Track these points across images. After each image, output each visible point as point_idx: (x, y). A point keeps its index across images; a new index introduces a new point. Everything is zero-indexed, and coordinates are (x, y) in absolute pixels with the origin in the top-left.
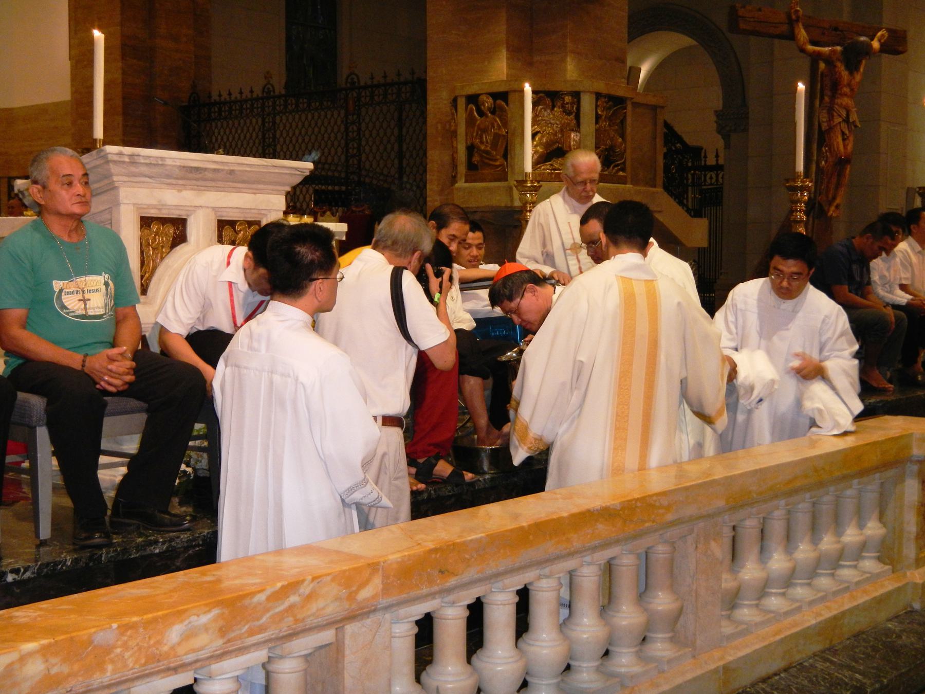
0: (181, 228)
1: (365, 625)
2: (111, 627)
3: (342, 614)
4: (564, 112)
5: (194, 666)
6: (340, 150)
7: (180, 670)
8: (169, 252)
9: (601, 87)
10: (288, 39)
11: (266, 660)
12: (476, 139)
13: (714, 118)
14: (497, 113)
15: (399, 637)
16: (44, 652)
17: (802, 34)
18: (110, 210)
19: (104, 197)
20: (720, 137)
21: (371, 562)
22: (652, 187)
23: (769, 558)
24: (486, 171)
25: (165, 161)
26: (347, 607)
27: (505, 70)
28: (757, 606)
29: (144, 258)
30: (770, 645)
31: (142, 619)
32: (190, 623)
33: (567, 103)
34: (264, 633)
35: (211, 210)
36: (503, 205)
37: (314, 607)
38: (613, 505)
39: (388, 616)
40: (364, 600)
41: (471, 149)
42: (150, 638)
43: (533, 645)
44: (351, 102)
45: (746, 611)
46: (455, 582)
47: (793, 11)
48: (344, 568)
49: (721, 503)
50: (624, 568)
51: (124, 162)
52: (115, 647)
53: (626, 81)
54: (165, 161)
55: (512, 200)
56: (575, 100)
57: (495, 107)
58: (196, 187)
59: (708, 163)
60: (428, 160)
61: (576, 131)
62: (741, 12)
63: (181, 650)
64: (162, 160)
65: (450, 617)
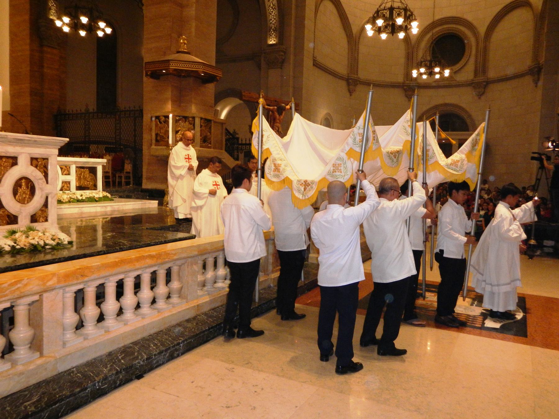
4: (189, 123)
9: (203, 116)
21: (52, 273)
24: (162, 143)
27: (170, 108)
37: (28, 288)
39: (61, 291)
40: (50, 285)
41: (157, 135)
44: (117, 117)
49: (196, 253)
62: (243, 94)
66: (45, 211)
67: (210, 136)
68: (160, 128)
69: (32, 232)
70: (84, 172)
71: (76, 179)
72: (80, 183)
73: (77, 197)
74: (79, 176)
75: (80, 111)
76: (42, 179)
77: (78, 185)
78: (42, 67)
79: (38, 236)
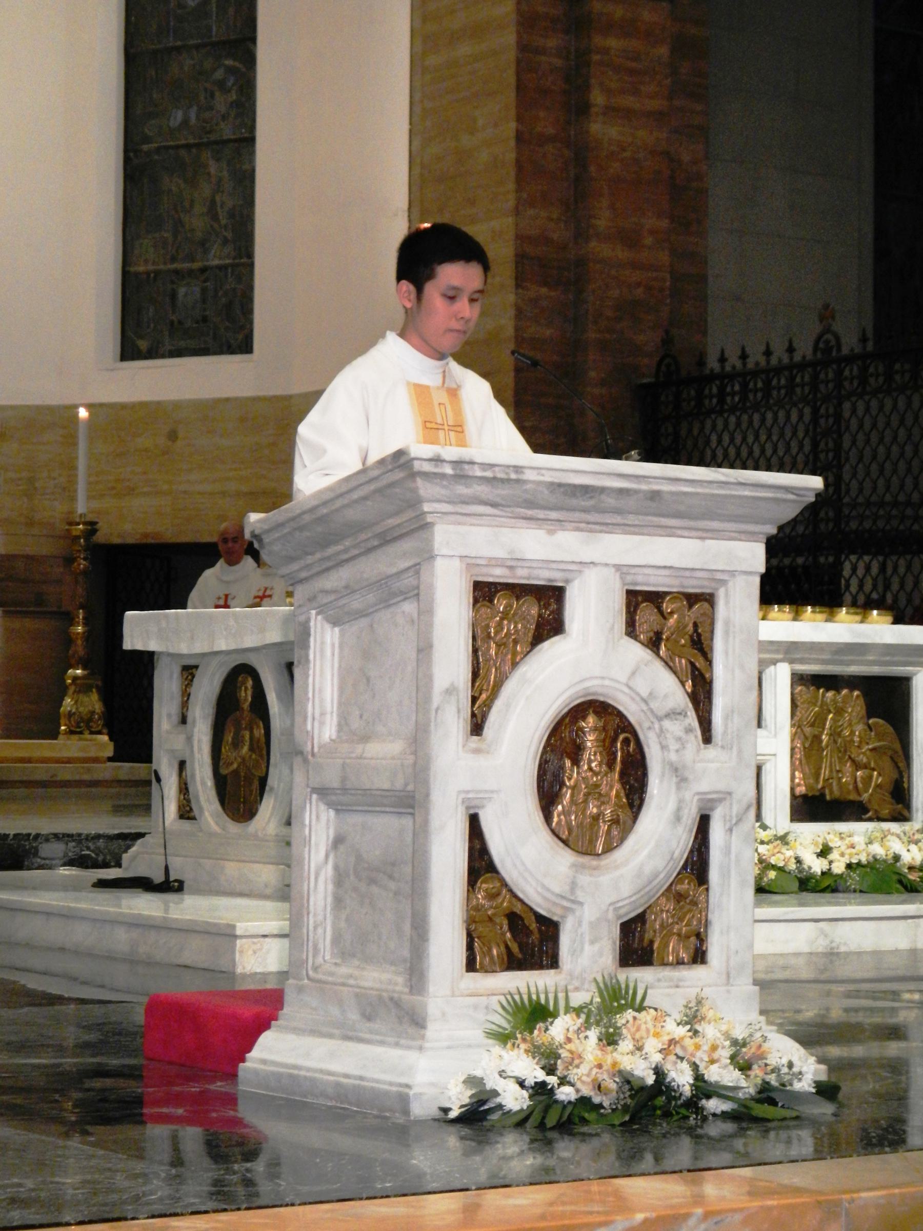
0: (554, 606)
8: (528, 652)
10: (880, 232)
18: (416, 569)
19: (407, 545)
25: (523, 472)
29: (478, 663)
35: (613, 570)
51: (443, 476)
54: (523, 472)
58: (583, 525)
66: (695, 903)
69: (629, 1014)
70: (839, 712)
71: (793, 749)
72: (817, 776)
73: (799, 861)
74: (808, 730)
76: (682, 714)
77: (800, 790)
78: (583, 109)
79: (666, 1038)
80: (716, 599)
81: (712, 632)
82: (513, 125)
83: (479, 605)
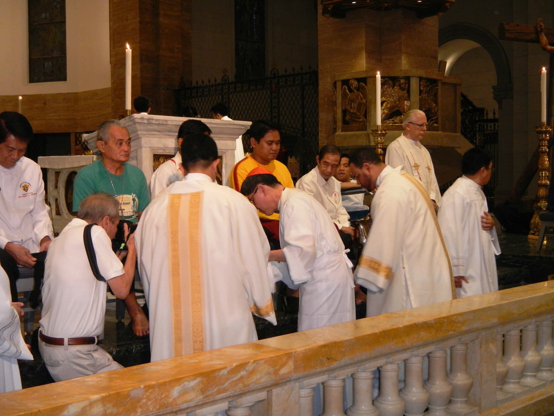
1: (284, 389)
2: (140, 387)
3: (271, 382)
4: (400, 89)
5: (186, 411)
6: (267, 114)
7: (179, 413)
9: (422, 73)
10: (237, 49)
11: (227, 408)
12: (348, 105)
13: (492, 91)
14: (360, 90)
15: (303, 397)
16: (103, 400)
17: (544, 39)
20: (496, 102)
22: (455, 133)
23: (526, 354)
25: (168, 122)
26: (274, 378)
27: (365, 65)
28: (518, 383)
30: (526, 406)
31: (157, 383)
32: (184, 386)
33: (402, 84)
34: (226, 392)
36: (364, 145)
37: (255, 378)
38: (430, 321)
39: (297, 384)
40: (283, 374)
41: (345, 112)
42: (162, 394)
43: (383, 404)
44: (274, 86)
45: (512, 386)
46: (337, 365)
47: (538, 26)
48: (272, 356)
49: (495, 320)
50: (437, 359)
51: (144, 123)
52: (142, 399)
53: (437, 70)
54: (168, 122)
55: (370, 142)
56: (407, 81)
57: (359, 87)
59: (489, 118)
60: (319, 119)
61: (408, 100)
62: (506, 27)
63: (179, 401)
64: (166, 122)
65: (334, 386)
67: (436, 108)
68: (350, 100)
75: (214, 82)
80: (223, 157)
81: (222, 167)
82: (139, 19)
83: (155, 161)
